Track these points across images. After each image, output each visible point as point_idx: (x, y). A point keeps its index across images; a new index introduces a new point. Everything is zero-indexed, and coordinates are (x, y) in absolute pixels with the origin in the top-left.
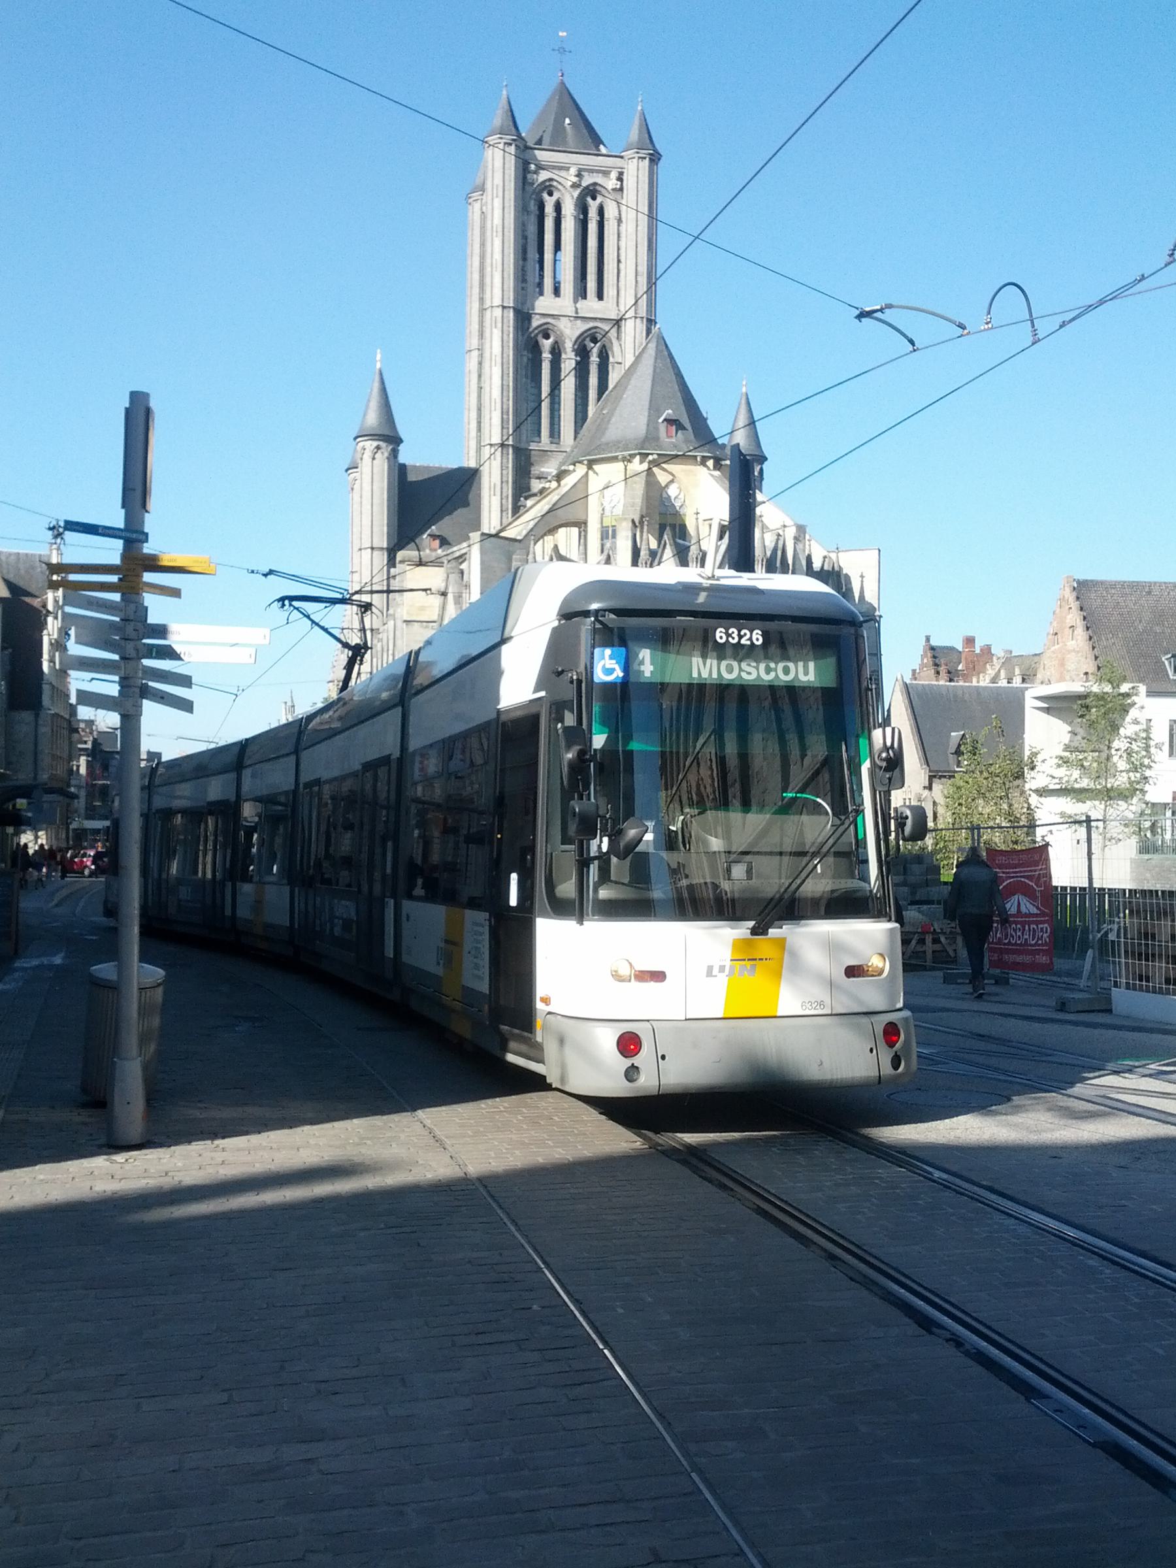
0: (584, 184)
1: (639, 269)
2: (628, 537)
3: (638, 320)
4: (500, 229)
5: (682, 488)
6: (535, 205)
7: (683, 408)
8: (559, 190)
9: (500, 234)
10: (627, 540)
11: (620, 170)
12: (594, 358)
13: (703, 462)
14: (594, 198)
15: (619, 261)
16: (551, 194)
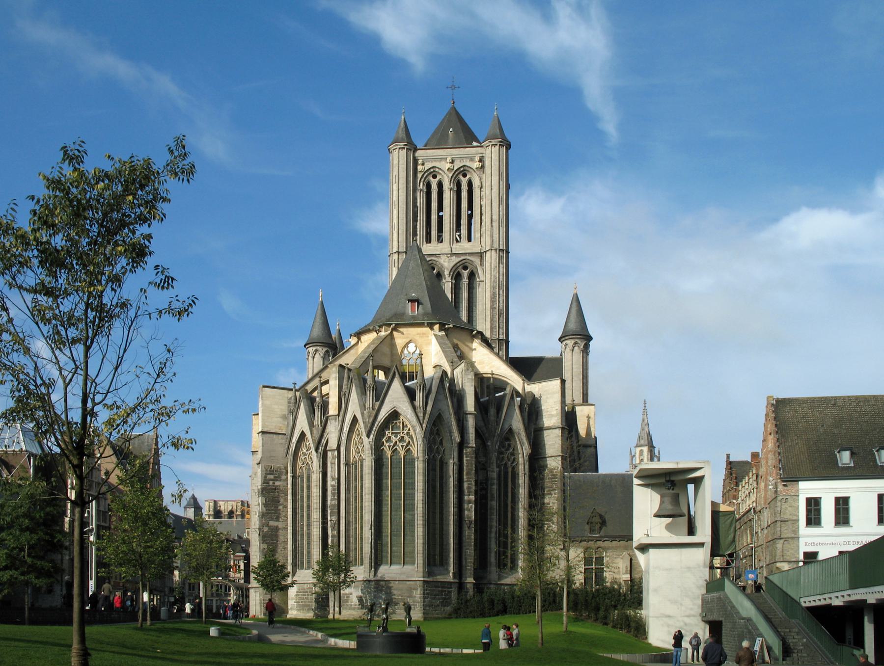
0: (456, 168)
1: (493, 217)
2: (336, 377)
3: (493, 251)
4: (397, 203)
5: (418, 345)
6: (423, 185)
7: (426, 292)
8: (440, 174)
9: (397, 206)
10: (336, 380)
11: (481, 155)
12: (465, 280)
13: (431, 326)
14: (465, 176)
15: (481, 214)
16: (435, 177)
